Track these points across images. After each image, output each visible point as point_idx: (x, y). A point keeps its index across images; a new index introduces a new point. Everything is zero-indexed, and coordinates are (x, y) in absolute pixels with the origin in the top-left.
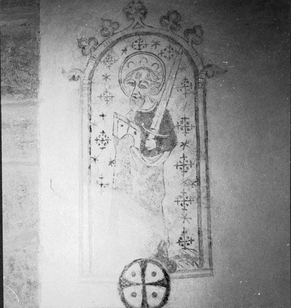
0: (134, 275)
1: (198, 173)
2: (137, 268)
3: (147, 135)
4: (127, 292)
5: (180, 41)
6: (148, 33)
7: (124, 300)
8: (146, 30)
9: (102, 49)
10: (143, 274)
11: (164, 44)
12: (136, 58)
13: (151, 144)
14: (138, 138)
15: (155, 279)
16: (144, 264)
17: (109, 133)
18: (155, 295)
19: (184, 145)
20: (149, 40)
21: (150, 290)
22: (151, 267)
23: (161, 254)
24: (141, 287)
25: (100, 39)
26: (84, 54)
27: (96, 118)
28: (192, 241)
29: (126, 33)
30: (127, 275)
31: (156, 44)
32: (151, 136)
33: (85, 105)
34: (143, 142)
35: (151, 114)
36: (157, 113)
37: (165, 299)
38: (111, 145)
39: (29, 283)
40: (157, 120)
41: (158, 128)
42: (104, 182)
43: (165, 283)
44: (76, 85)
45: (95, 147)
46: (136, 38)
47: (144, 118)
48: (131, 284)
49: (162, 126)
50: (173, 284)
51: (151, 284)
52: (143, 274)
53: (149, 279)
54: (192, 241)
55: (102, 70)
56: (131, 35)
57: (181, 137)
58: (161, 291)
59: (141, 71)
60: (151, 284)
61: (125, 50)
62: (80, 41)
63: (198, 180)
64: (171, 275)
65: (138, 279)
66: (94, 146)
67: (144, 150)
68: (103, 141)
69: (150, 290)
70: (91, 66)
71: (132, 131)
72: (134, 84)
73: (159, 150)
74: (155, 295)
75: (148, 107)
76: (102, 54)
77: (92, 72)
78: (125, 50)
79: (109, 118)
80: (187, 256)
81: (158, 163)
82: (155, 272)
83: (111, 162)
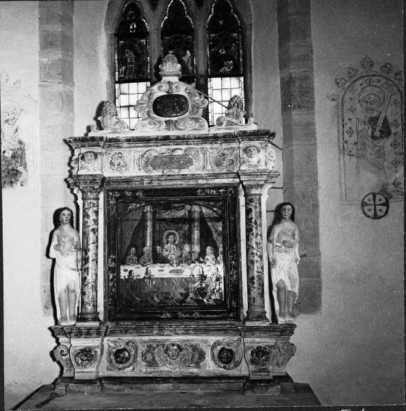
0: (370, 200)
2: (371, 197)
4: (366, 208)
5: (393, 79)
6: (374, 75)
8: (373, 73)
10: (374, 200)
11: (383, 81)
12: (368, 89)
13: (377, 134)
14: (370, 131)
16: (374, 195)
17: (354, 129)
18: (381, 210)
19: (395, 134)
20: (375, 79)
21: (378, 208)
22: (378, 197)
23: (384, 191)
24: (373, 207)
25: (347, 79)
27: (346, 119)
28: (400, 183)
29: (362, 75)
30: (366, 200)
31: (379, 81)
32: (377, 130)
33: (340, 113)
34: (373, 133)
35: (377, 118)
36: (380, 118)
37: (386, 213)
40: (380, 121)
41: (381, 125)
43: (386, 204)
44: (334, 103)
45: (347, 137)
46: (367, 78)
47: (373, 121)
48: (368, 205)
49: (383, 124)
51: (379, 205)
52: (374, 200)
53: (378, 202)
54: (400, 183)
56: (364, 76)
57: (393, 130)
58: (384, 209)
59: (371, 96)
60: (379, 205)
64: (390, 201)
65: (372, 202)
67: (373, 137)
70: (343, 93)
71: (366, 127)
72: (367, 102)
73: (381, 137)
75: (375, 114)
76: (348, 88)
77: (343, 97)
78: (362, 85)
79: (354, 120)
80: (398, 191)
81: (382, 143)
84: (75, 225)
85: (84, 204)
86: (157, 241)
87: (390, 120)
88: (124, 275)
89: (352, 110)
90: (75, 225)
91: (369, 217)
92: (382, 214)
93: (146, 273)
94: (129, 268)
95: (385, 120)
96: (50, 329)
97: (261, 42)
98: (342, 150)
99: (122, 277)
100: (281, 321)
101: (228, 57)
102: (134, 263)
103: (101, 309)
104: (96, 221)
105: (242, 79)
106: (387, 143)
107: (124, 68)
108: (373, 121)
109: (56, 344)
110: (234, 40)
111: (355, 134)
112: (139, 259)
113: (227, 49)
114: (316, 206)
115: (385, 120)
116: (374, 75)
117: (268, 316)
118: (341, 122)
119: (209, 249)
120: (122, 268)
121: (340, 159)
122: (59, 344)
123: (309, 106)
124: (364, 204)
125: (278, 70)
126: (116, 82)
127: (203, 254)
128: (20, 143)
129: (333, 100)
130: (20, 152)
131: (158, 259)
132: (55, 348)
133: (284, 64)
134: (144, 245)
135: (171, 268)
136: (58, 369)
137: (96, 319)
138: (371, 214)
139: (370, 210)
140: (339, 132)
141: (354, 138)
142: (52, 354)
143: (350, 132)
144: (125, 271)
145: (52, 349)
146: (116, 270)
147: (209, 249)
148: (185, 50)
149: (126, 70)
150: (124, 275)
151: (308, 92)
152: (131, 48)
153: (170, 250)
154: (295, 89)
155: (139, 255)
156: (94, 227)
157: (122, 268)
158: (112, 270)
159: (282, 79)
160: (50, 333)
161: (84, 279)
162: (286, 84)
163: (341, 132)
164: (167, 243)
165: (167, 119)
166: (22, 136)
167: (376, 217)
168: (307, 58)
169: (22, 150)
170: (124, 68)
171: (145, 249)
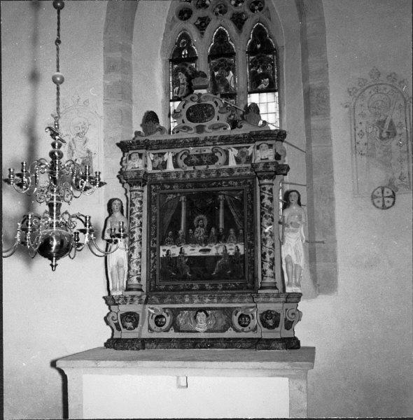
1: (408, 147)
2: (380, 190)
3: (382, 131)
4: (376, 201)
6: (381, 84)
7: (374, 204)
8: (381, 82)
9: (359, 92)
10: (383, 192)
11: (389, 88)
12: (376, 96)
13: (384, 135)
14: (378, 133)
15: (389, 195)
17: (365, 131)
18: (388, 202)
20: (382, 87)
21: (386, 199)
22: (386, 190)
23: (391, 183)
24: (381, 199)
26: (350, 95)
27: (357, 122)
30: (375, 193)
31: (385, 89)
32: (384, 131)
33: (352, 117)
34: (380, 134)
35: (384, 122)
37: (394, 203)
38: (365, 136)
39: (330, 198)
40: (387, 123)
42: (363, 153)
43: (393, 196)
44: (347, 109)
45: (358, 139)
46: (376, 86)
47: (381, 123)
48: (377, 197)
50: (397, 197)
52: (383, 192)
53: (386, 194)
55: (359, 102)
56: (373, 85)
57: (398, 131)
58: (391, 200)
61: (370, 92)
62: (348, 89)
63: (408, 150)
65: (380, 195)
66: (357, 136)
67: (381, 138)
68: (361, 134)
69: (386, 199)
71: (375, 129)
72: (375, 108)
74: (388, 202)
75: (382, 118)
77: (355, 103)
78: (370, 92)
79: (364, 125)
82: (388, 192)
83: (366, 144)
84: (125, 213)
85: (131, 196)
86: (190, 225)
87: (396, 122)
88: (163, 254)
89: (363, 115)
90: (125, 213)
91: (378, 207)
92: (390, 205)
93: (180, 253)
94: (167, 248)
95: (391, 123)
96: (104, 297)
97: (289, 64)
98: (355, 150)
99: (161, 256)
100: (288, 290)
101: (265, 75)
102: (172, 244)
103: (144, 282)
104: (140, 209)
105: (277, 93)
106: (393, 143)
107: (177, 88)
108: (381, 123)
109: (109, 311)
110: (270, 60)
111: (365, 136)
112: (176, 242)
113: (264, 68)
114: (332, 199)
115: (391, 123)
116: (381, 84)
117: (279, 286)
118: (353, 126)
119: (232, 231)
120: (161, 248)
121: (352, 157)
122: (111, 311)
123: (326, 113)
124: (373, 197)
125: (302, 84)
126: (171, 101)
127: (227, 234)
128: (89, 152)
129: (346, 107)
130: (88, 160)
131: (189, 240)
132: (108, 314)
133: (305, 78)
134: (179, 229)
135: (201, 248)
136: (111, 331)
137: (141, 290)
138: (380, 205)
139: (379, 202)
140: (351, 134)
141: (365, 140)
142: (105, 319)
143: (361, 134)
144: (164, 250)
145: (105, 315)
146: (155, 250)
147: (232, 231)
148: (228, 70)
149: (179, 90)
150: (163, 254)
151: (325, 101)
152: (183, 71)
153: (200, 232)
154: (313, 99)
155: (176, 235)
156: (139, 213)
157: (161, 248)
158: (152, 250)
159: (304, 91)
160: (104, 301)
161: (130, 257)
162: (307, 94)
163: (353, 135)
164: (198, 227)
165: (198, 124)
166: (90, 146)
167: (384, 207)
168: (323, 72)
169: (90, 158)
170: (177, 88)
171: (180, 232)
